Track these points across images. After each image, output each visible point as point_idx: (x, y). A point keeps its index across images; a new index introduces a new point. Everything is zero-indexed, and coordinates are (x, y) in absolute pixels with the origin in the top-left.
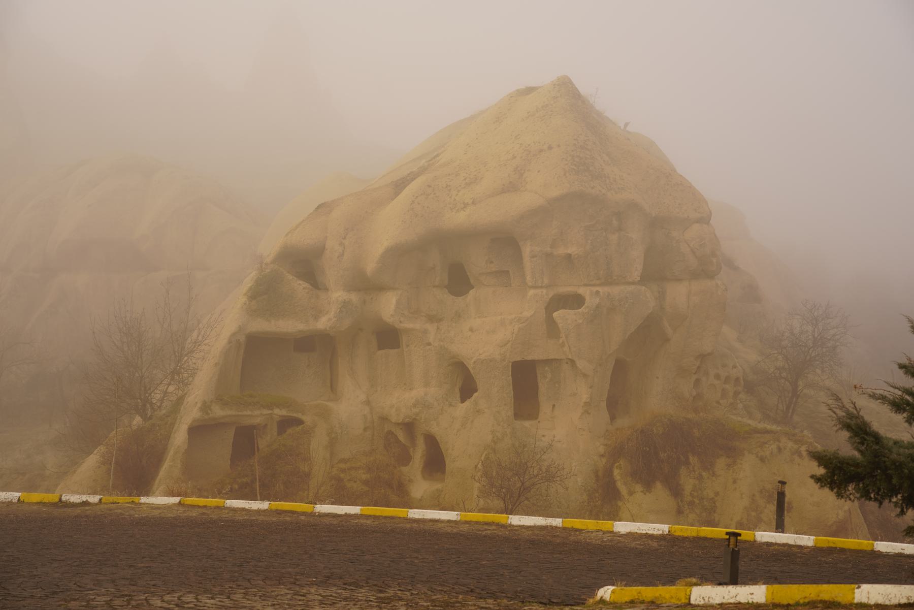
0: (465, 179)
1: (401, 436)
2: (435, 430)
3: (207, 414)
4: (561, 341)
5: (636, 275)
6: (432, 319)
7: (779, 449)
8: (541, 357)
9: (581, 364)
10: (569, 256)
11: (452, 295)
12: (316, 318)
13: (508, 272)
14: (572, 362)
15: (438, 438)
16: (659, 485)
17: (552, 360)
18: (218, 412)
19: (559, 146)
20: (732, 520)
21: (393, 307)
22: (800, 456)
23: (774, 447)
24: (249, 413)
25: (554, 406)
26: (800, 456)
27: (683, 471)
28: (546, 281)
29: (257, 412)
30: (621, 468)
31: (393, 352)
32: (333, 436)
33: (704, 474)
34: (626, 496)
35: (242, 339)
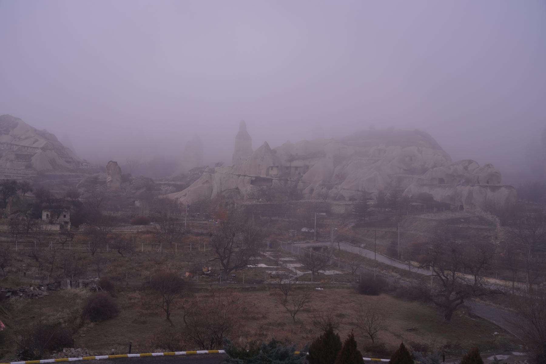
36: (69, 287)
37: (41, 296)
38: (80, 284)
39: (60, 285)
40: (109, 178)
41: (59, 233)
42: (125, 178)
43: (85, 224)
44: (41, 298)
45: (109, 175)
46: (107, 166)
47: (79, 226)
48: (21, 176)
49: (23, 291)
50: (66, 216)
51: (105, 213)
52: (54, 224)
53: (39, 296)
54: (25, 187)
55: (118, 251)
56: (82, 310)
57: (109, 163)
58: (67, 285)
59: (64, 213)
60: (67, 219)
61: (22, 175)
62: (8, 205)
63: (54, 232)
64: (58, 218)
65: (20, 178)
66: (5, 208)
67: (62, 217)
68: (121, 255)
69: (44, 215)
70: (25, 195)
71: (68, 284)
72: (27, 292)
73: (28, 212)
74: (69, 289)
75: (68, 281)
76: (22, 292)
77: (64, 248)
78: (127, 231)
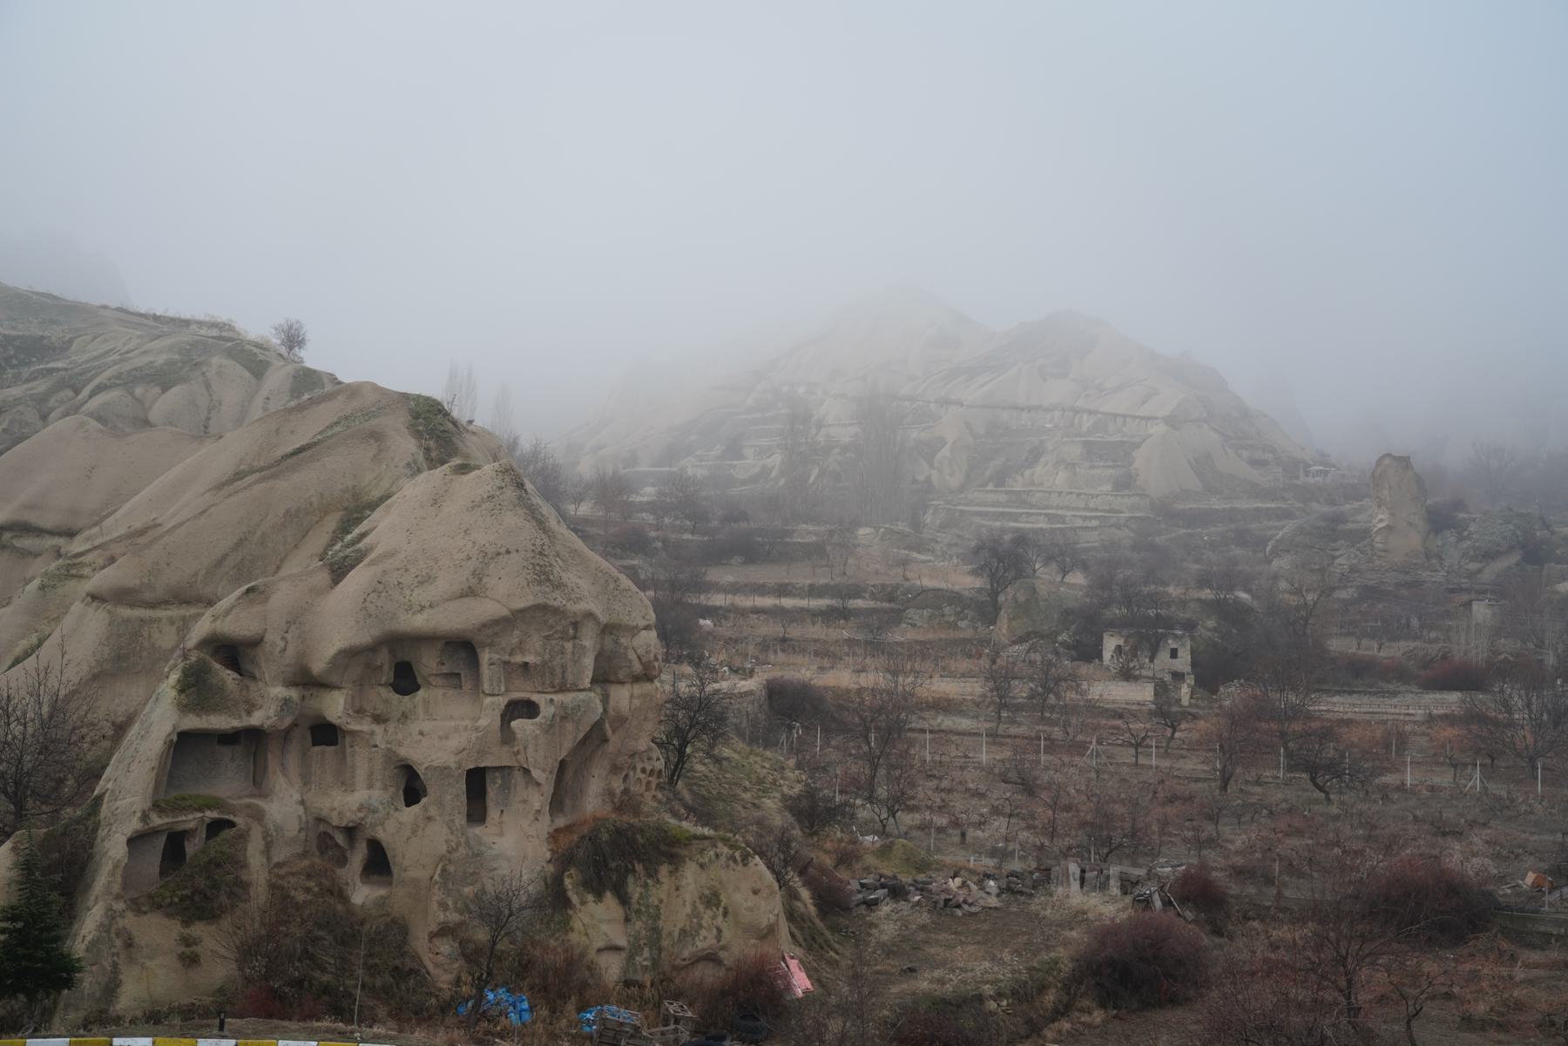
0: (417, 577)
1: (340, 839)
2: (381, 835)
3: (148, 824)
4: (516, 749)
5: (587, 683)
6: (379, 719)
7: (717, 856)
8: (494, 765)
9: (536, 773)
10: (526, 664)
11: (397, 693)
12: (249, 713)
13: (459, 674)
14: (526, 772)
15: (384, 845)
16: (608, 894)
17: (505, 767)
18: (157, 821)
19: (517, 551)
20: (675, 926)
21: (341, 708)
22: (735, 861)
23: (712, 853)
24: (184, 818)
25: (502, 811)
26: (735, 861)
27: (630, 879)
28: (503, 689)
29: (190, 817)
30: (572, 877)
31: (331, 749)
32: (269, 839)
33: (649, 881)
34: (578, 906)
35: (175, 738)
36: (1075, 886)
37: (973, 909)
38: (1112, 882)
39: (1048, 880)
40: (1380, 517)
41: (1150, 710)
42: (1441, 520)
43: (1242, 681)
44: (972, 914)
45: (1379, 506)
46: (1373, 474)
47: (1222, 689)
48: (1096, 518)
49: (922, 889)
50: (1180, 654)
51: (1339, 645)
52: (1136, 678)
53: (966, 907)
54: (1065, 556)
55: (1313, 780)
56: (1070, 965)
57: (1379, 461)
58: (1068, 881)
59: (1170, 642)
60: (1183, 662)
61: (1098, 514)
62: (1002, 612)
63: (1134, 707)
64: (1152, 660)
65: (1094, 523)
66: (994, 623)
67: (1163, 656)
68: (1323, 795)
69: (1110, 644)
70: (1067, 579)
71: (1071, 878)
72: (930, 892)
73: (1060, 638)
74: (1072, 895)
75: (1074, 868)
76: (918, 892)
77: (1140, 762)
78: (1393, 711)
